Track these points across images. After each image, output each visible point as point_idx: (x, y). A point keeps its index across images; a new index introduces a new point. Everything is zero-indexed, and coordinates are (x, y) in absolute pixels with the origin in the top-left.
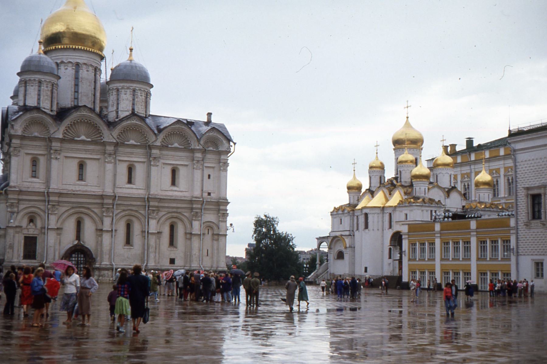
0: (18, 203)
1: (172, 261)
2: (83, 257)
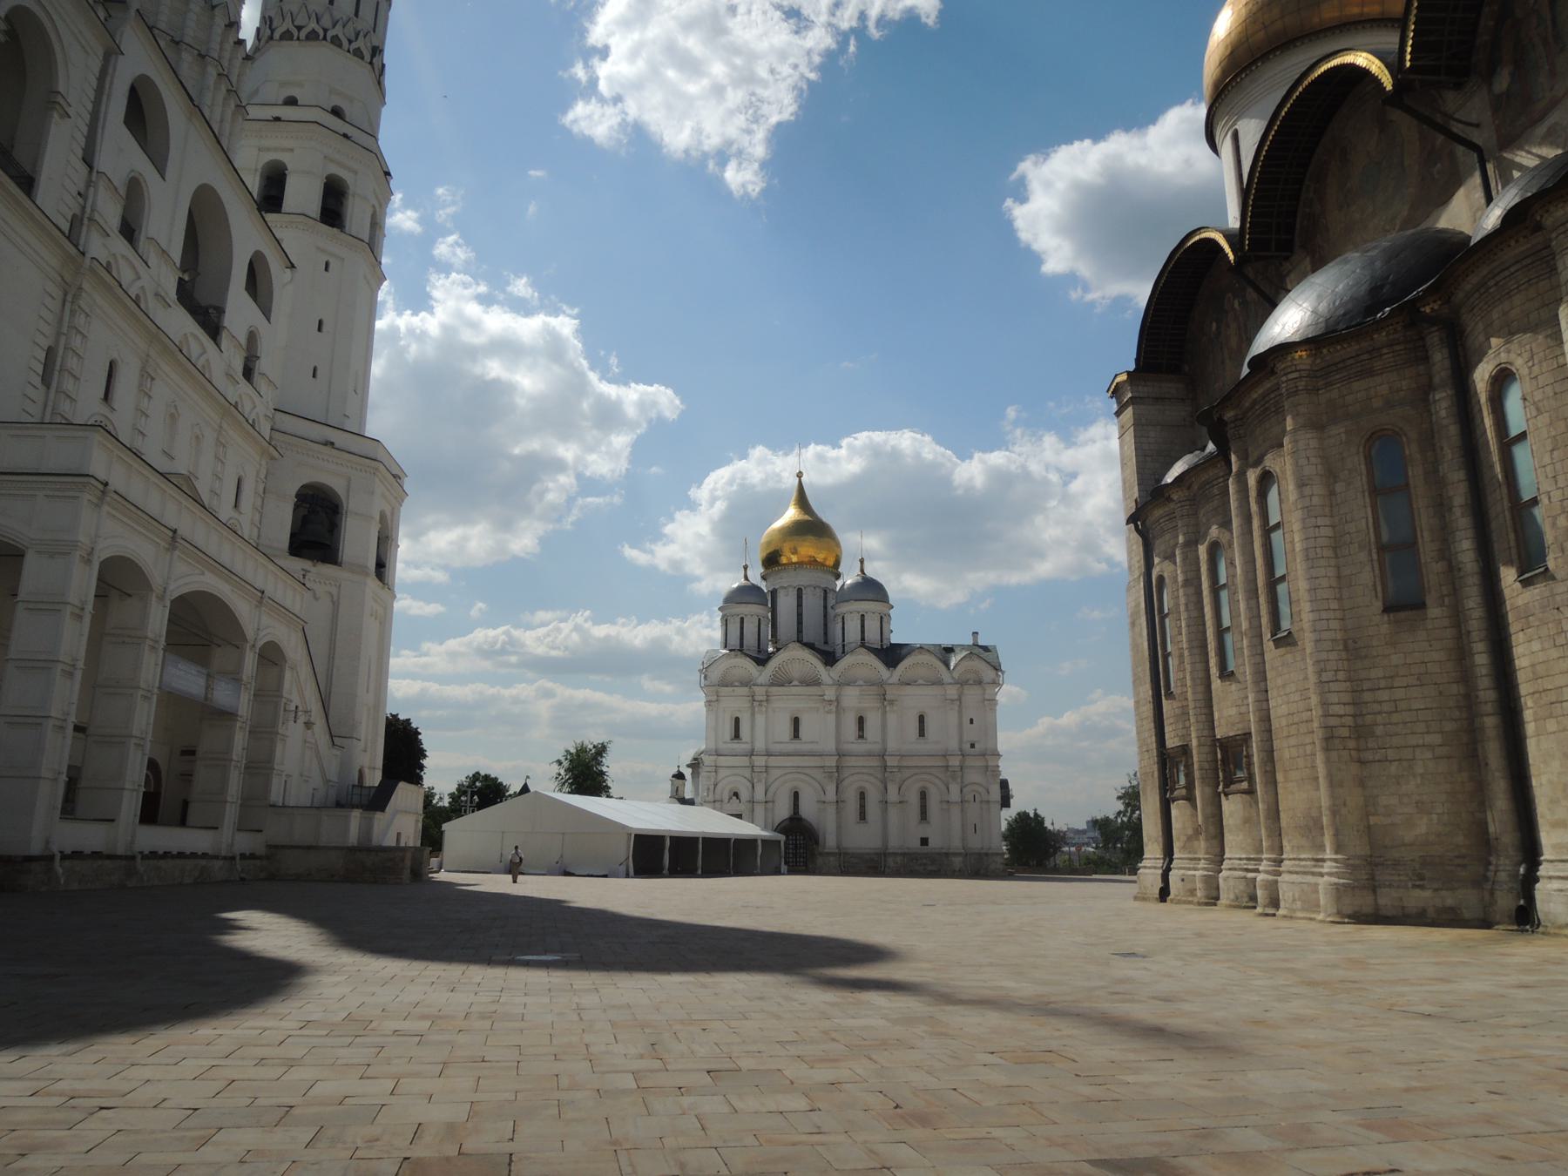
0: (716, 772)
1: (924, 841)
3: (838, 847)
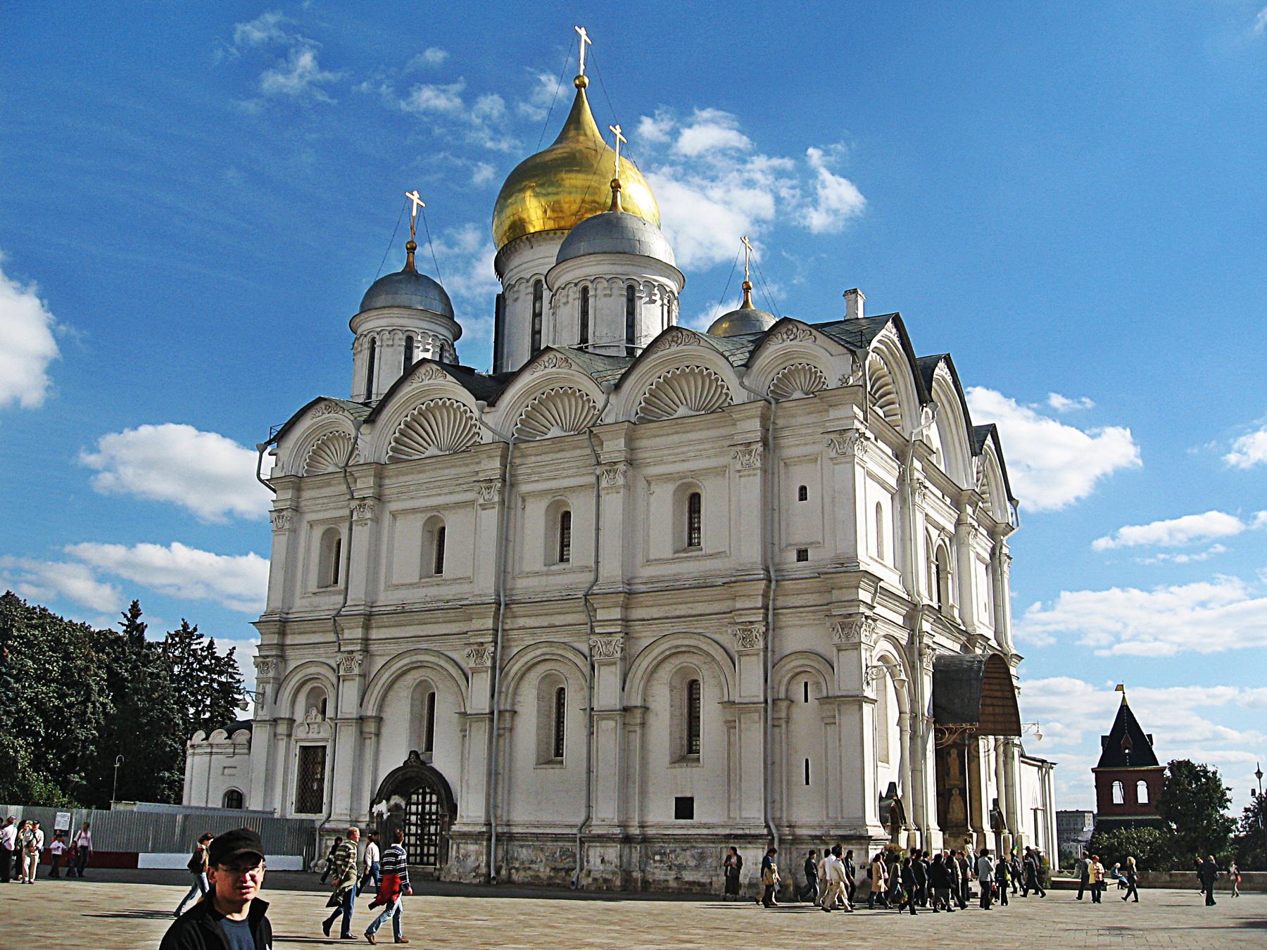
0: (282, 658)
1: (684, 808)
2: (437, 803)
3: (488, 824)
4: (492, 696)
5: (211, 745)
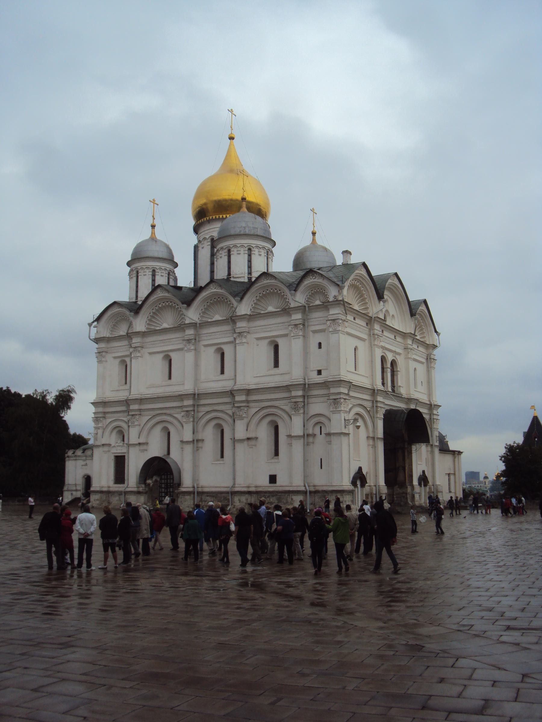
1: (273, 479)
4: (194, 433)
5: (76, 456)
